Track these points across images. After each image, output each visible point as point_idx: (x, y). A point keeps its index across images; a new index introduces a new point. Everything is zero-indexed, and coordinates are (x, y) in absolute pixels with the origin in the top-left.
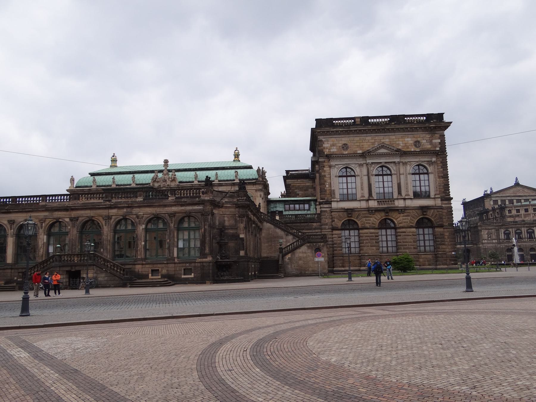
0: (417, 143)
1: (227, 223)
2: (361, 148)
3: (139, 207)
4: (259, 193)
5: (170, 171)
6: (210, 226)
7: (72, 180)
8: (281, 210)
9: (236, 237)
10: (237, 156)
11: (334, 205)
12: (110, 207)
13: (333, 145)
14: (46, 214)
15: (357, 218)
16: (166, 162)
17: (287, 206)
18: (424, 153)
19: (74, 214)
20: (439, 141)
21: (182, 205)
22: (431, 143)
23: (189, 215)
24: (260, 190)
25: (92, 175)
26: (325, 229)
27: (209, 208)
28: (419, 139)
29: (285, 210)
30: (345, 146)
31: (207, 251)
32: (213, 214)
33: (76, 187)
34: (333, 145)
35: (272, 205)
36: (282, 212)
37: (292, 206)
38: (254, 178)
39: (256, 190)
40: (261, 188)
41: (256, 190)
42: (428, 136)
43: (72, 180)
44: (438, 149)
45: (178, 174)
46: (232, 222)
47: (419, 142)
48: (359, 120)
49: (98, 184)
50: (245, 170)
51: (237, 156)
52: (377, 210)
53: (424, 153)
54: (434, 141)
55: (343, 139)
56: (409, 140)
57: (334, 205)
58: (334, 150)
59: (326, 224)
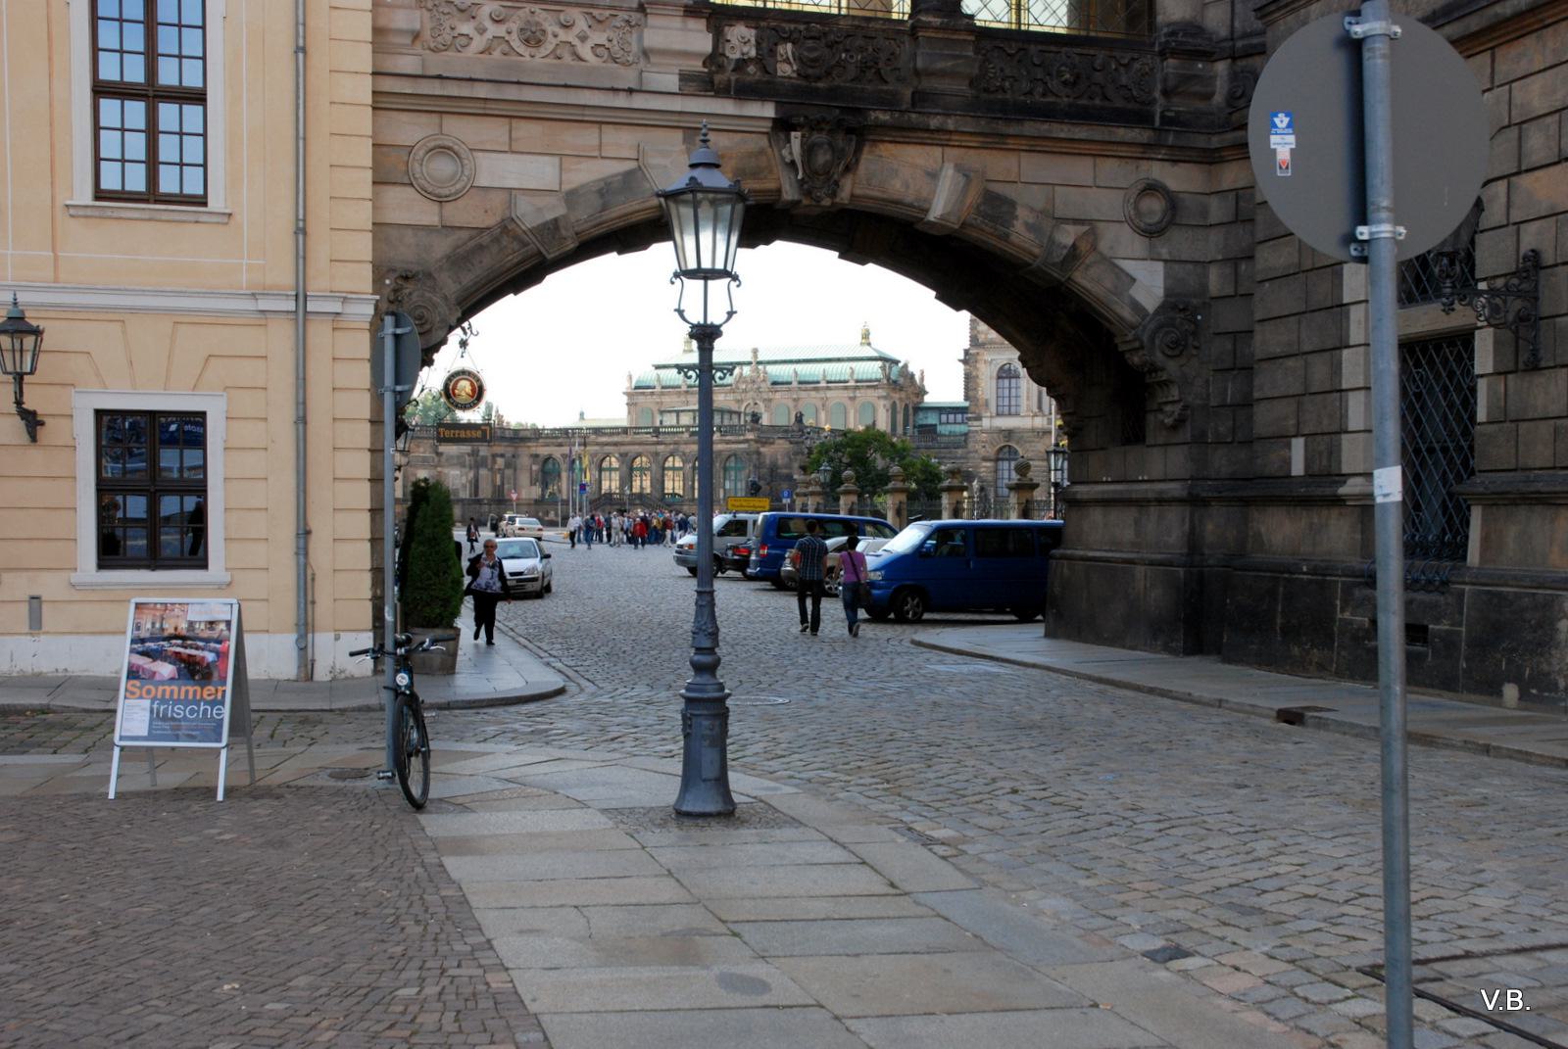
1: (780, 462)
3: (686, 444)
4: (882, 402)
6: (755, 466)
7: (630, 377)
8: (934, 422)
9: (789, 478)
10: (866, 336)
11: (986, 423)
12: (658, 443)
14: (597, 448)
15: (1018, 443)
16: (755, 352)
17: (944, 418)
19: (623, 449)
23: (734, 455)
24: (885, 398)
25: (658, 367)
26: (974, 458)
27: (754, 446)
29: (941, 423)
32: (758, 453)
33: (636, 388)
35: (921, 415)
36: (935, 425)
37: (951, 417)
38: (874, 377)
39: (879, 398)
40: (884, 394)
41: (879, 398)
43: (630, 377)
45: (770, 369)
46: (786, 459)
49: (664, 384)
50: (869, 363)
51: (866, 336)
57: (986, 423)
59: (976, 452)
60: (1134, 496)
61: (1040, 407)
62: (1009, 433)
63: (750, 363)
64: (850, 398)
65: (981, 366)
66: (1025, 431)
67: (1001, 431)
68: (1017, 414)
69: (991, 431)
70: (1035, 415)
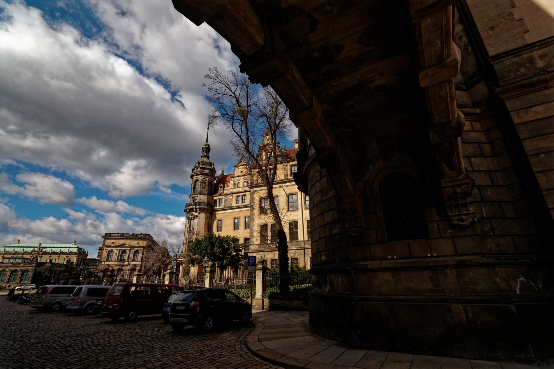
0: (138, 243)
1: (42, 272)
2: (118, 243)
4: (76, 258)
5: (41, 247)
13: (109, 242)
18: (140, 247)
20: (146, 243)
21: (25, 267)
22: (143, 243)
28: (139, 242)
30: (113, 243)
31: (30, 280)
34: (109, 242)
42: (143, 241)
44: (145, 245)
47: (139, 243)
48: (120, 234)
52: (117, 265)
53: (140, 247)
54: (144, 243)
55: (113, 240)
56: (136, 242)
57: (103, 263)
58: (109, 244)
60: (432, 264)
61: (118, 259)
62: (109, 265)
63: (37, 247)
64: (67, 256)
65: (104, 250)
66: (112, 265)
67: (107, 265)
68: (111, 261)
69: (104, 265)
70: (115, 261)
